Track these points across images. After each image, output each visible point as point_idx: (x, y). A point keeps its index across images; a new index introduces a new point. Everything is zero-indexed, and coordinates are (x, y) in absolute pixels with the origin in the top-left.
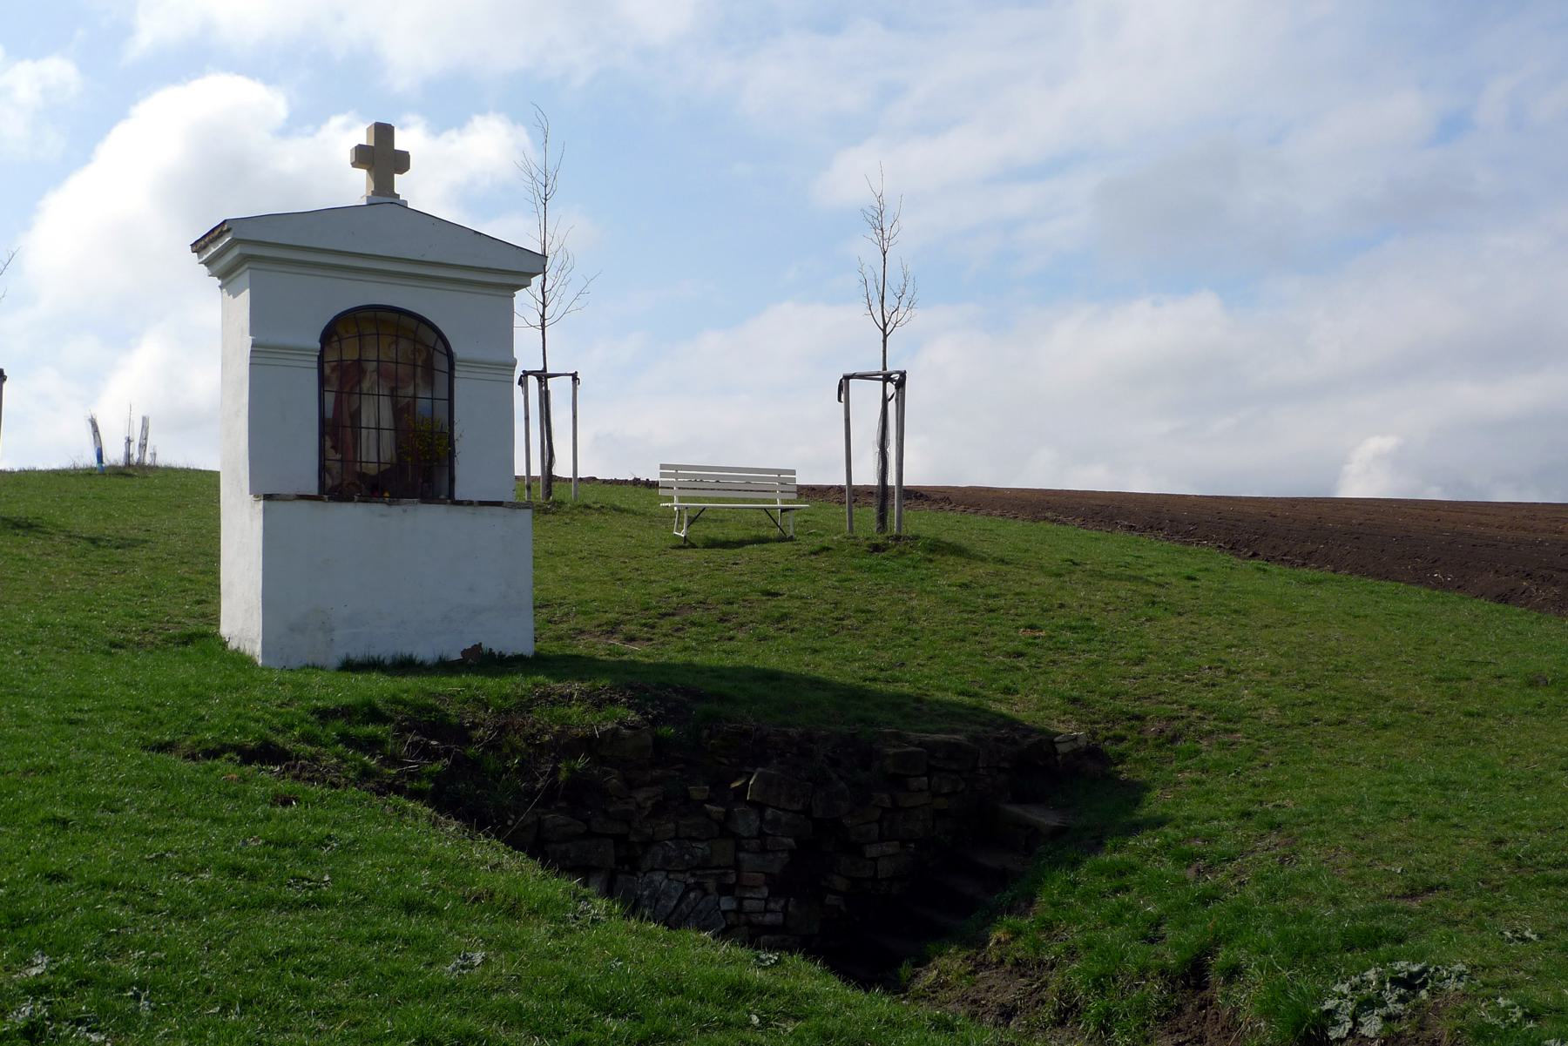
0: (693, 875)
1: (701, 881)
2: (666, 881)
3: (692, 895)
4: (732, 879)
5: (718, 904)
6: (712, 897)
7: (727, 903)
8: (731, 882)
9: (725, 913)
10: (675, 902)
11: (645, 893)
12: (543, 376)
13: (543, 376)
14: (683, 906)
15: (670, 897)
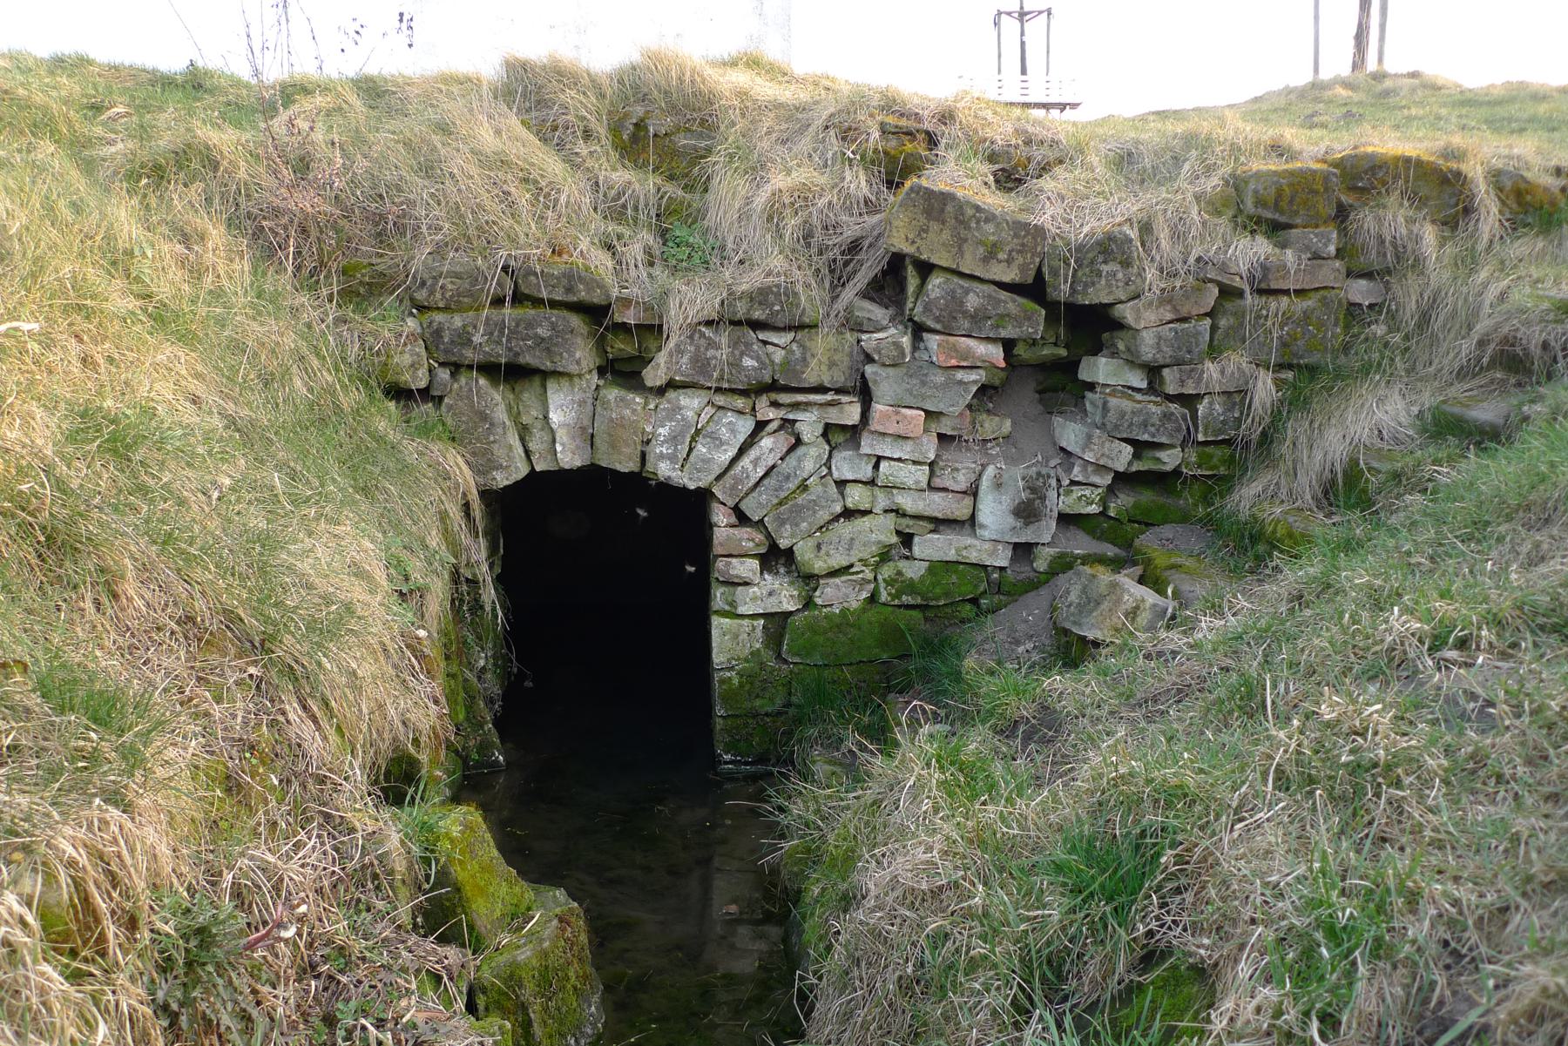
0: (775, 404)
1: (791, 416)
2: (710, 410)
3: (766, 442)
4: (851, 413)
5: (828, 464)
6: (813, 451)
7: (845, 466)
8: (850, 423)
9: (841, 484)
10: (731, 453)
11: (661, 430)
12: (1022, 15)
13: (1022, 15)
14: (746, 462)
15: (719, 443)
